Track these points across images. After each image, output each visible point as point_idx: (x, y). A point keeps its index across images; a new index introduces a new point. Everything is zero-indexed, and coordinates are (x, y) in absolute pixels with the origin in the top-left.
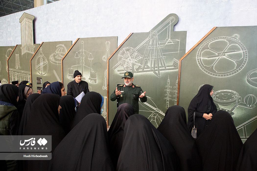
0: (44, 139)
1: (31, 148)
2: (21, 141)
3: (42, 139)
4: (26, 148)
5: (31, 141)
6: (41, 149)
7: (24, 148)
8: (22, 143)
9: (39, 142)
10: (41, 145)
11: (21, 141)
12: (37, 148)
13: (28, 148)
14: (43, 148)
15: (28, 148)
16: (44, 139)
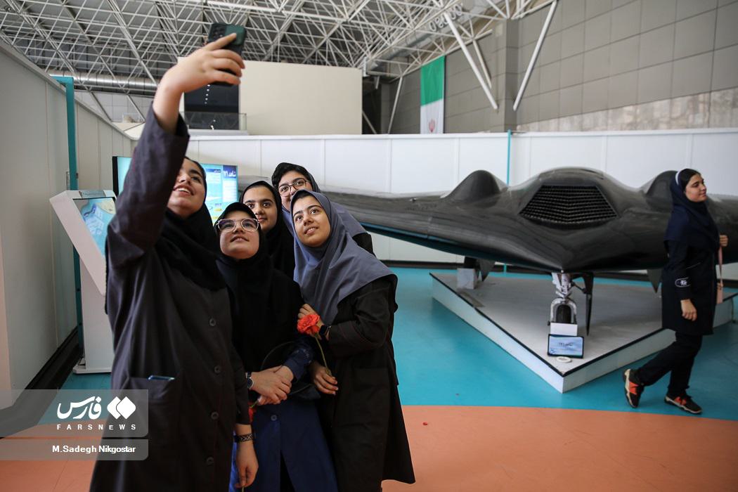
0: (126, 399)
1: (90, 427)
2: (60, 404)
3: (121, 399)
4: (74, 427)
5: (88, 405)
6: (116, 427)
7: (69, 427)
8: (63, 411)
9: (111, 408)
10: (117, 416)
11: (60, 404)
12: (106, 427)
13: (80, 427)
14: (122, 427)
15: (80, 427)
16: (126, 399)
